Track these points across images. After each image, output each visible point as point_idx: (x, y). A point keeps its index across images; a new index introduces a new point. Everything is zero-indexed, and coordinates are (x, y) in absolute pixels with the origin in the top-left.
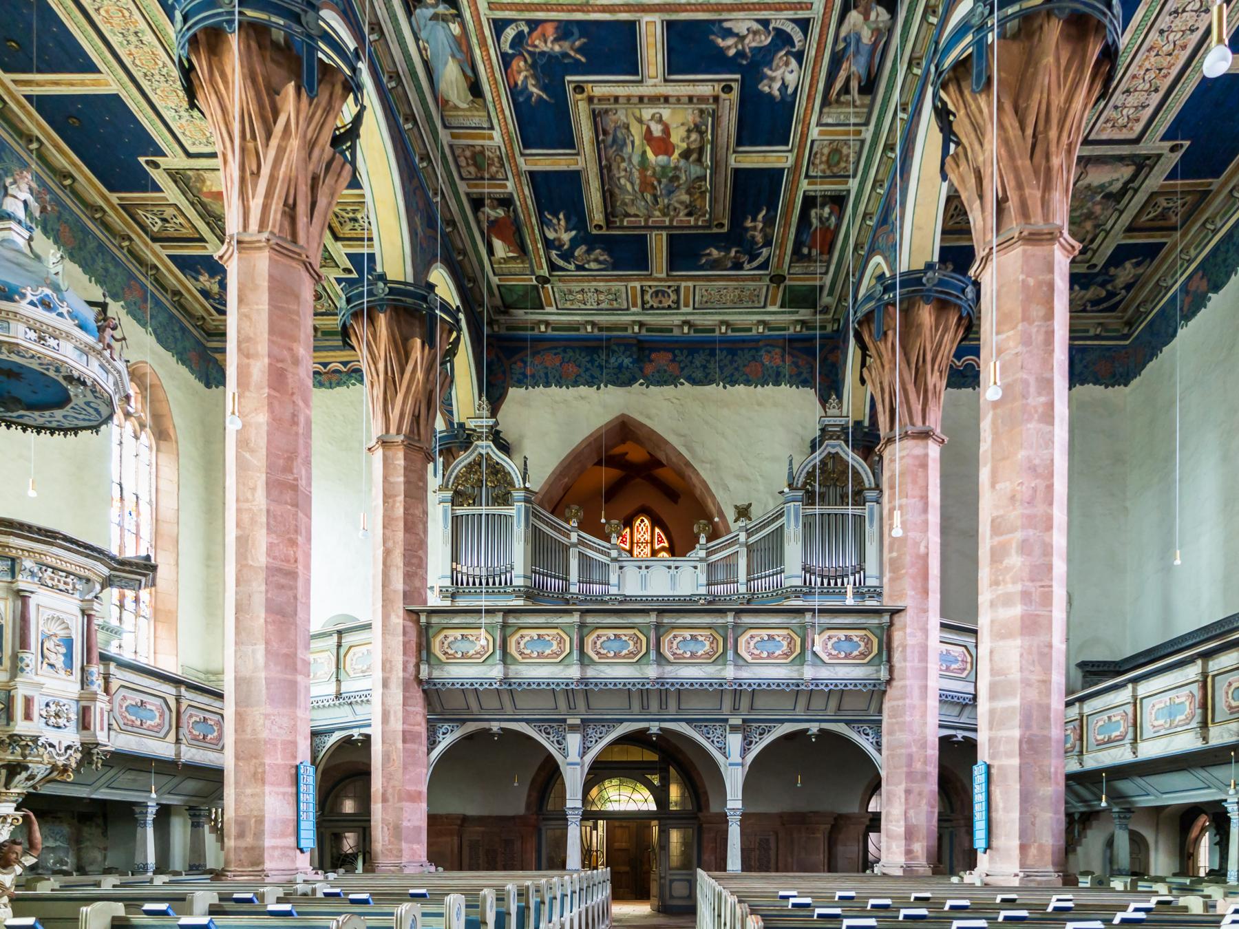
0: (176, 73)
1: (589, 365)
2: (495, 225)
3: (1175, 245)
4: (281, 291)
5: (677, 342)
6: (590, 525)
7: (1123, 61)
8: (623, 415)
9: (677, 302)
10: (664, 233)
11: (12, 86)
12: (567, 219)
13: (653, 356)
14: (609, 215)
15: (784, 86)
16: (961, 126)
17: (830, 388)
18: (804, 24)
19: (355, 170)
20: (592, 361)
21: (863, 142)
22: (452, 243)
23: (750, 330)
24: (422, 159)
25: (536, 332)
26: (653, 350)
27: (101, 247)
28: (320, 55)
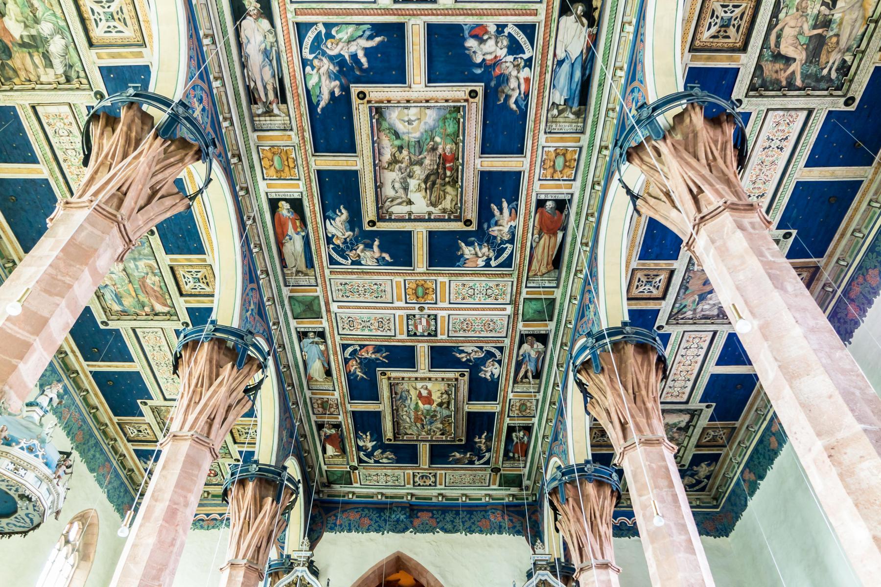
0: (171, 359)
1: (378, 519)
2: (328, 438)
3: (727, 455)
4: (191, 462)
5: (434, 506)
7: (669, 363)
9: (435, 482)
10: (428, 444)
11: (85, 367)
13: (419, 514)
15: (492, 374)
16: (592, 389)
17: (536, 535)
18: (501, 349)
19: (254, 404)
20: (380, 517)
21: (538, 401)
22: (303, 447)
23: (481, 499)
24: (293, 404)
25: (346, 498)
27: (97, 444)
28: (249, 352)
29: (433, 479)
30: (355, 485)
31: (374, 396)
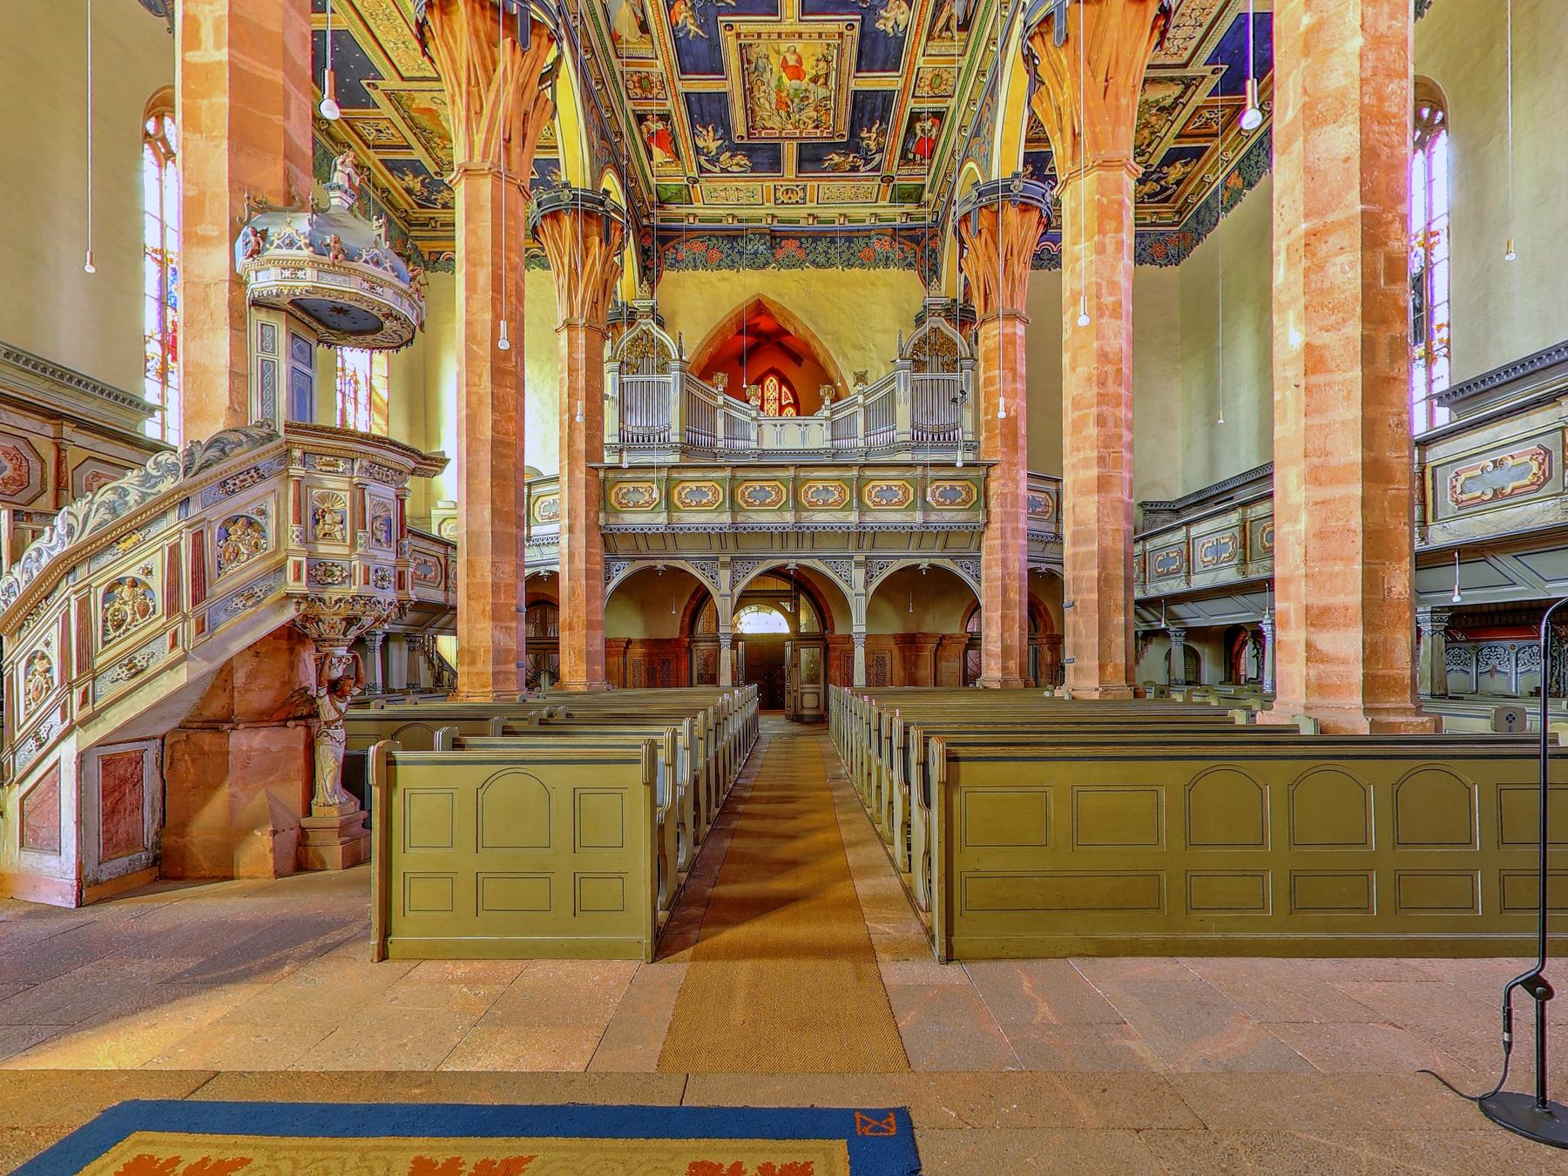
3: (1217, 149)
6: (734, 390)
12: (715, 131)
14: (750, 130)
20: (732, 248)
26: (782, 238)
29: (801, 194)
30: (696, 204)
31: (718, 69)
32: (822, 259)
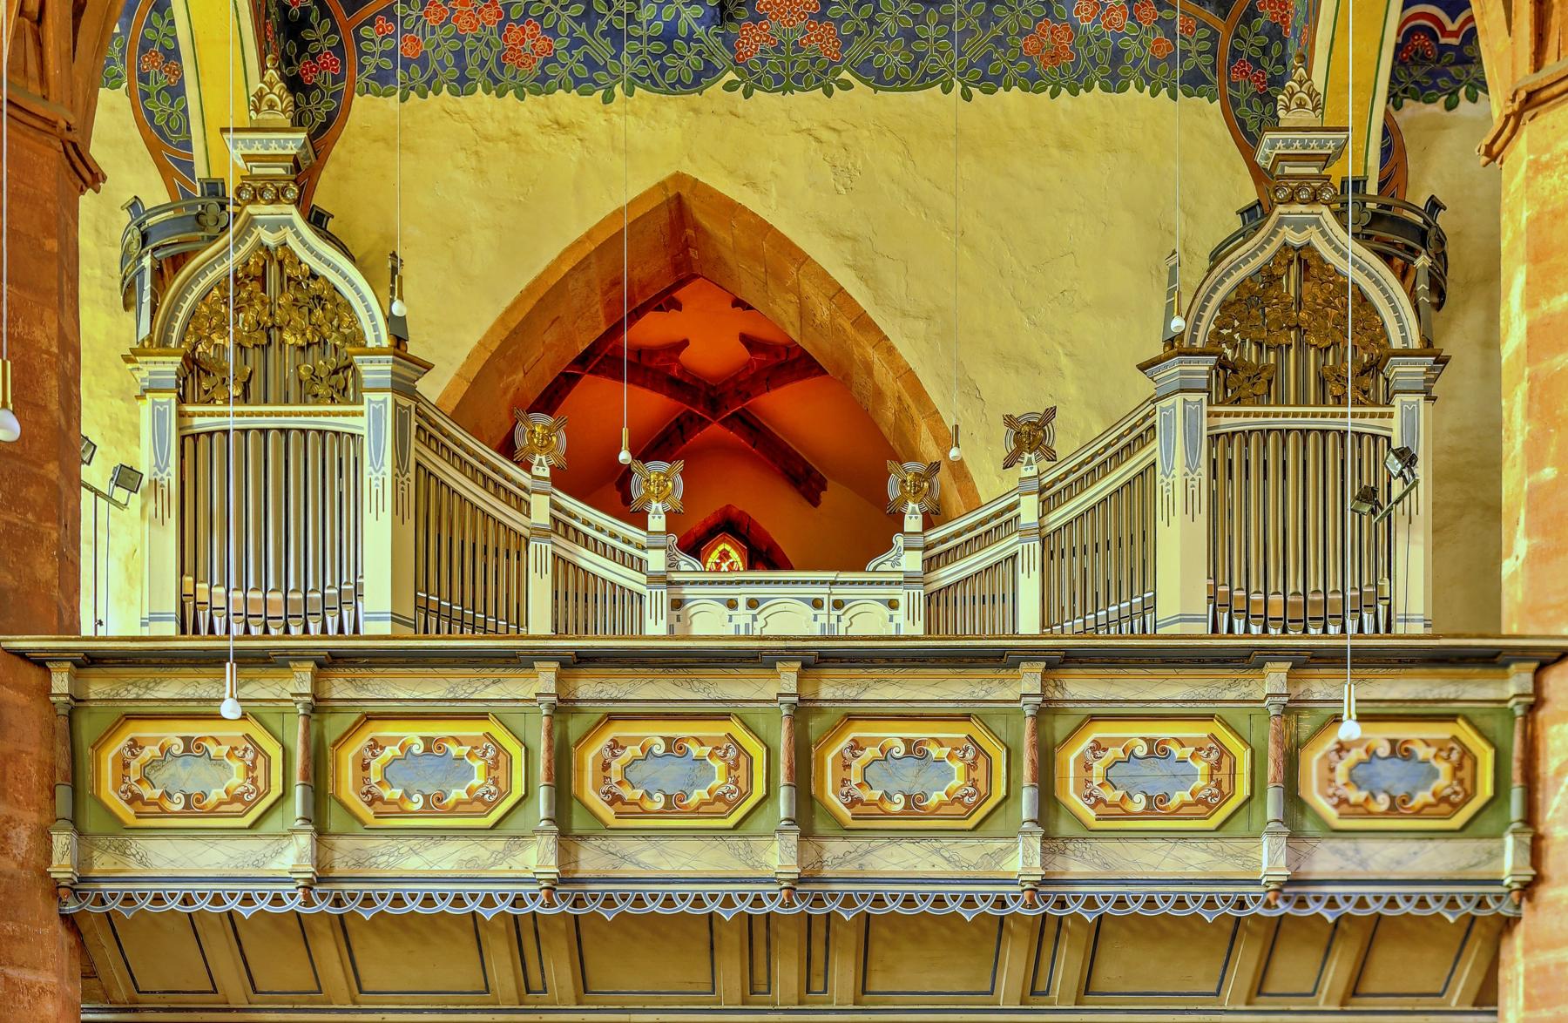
1: (581, 31)
8: (679, 178)
32: (894, 58)
